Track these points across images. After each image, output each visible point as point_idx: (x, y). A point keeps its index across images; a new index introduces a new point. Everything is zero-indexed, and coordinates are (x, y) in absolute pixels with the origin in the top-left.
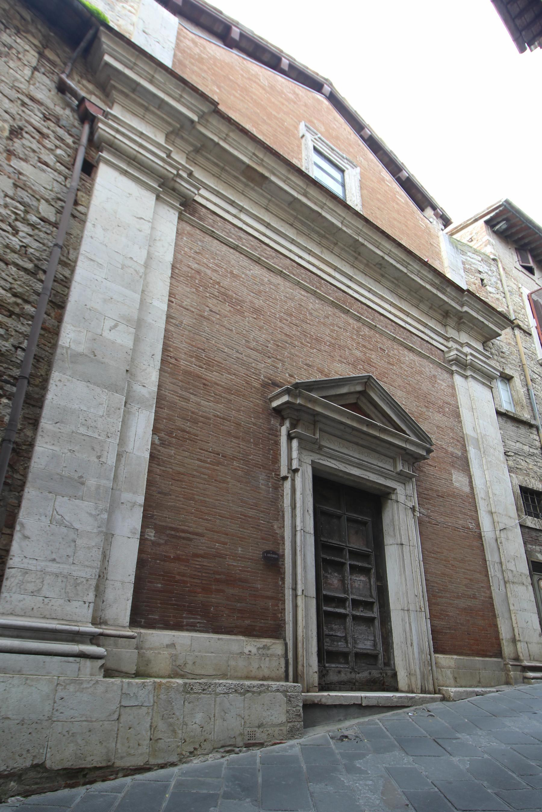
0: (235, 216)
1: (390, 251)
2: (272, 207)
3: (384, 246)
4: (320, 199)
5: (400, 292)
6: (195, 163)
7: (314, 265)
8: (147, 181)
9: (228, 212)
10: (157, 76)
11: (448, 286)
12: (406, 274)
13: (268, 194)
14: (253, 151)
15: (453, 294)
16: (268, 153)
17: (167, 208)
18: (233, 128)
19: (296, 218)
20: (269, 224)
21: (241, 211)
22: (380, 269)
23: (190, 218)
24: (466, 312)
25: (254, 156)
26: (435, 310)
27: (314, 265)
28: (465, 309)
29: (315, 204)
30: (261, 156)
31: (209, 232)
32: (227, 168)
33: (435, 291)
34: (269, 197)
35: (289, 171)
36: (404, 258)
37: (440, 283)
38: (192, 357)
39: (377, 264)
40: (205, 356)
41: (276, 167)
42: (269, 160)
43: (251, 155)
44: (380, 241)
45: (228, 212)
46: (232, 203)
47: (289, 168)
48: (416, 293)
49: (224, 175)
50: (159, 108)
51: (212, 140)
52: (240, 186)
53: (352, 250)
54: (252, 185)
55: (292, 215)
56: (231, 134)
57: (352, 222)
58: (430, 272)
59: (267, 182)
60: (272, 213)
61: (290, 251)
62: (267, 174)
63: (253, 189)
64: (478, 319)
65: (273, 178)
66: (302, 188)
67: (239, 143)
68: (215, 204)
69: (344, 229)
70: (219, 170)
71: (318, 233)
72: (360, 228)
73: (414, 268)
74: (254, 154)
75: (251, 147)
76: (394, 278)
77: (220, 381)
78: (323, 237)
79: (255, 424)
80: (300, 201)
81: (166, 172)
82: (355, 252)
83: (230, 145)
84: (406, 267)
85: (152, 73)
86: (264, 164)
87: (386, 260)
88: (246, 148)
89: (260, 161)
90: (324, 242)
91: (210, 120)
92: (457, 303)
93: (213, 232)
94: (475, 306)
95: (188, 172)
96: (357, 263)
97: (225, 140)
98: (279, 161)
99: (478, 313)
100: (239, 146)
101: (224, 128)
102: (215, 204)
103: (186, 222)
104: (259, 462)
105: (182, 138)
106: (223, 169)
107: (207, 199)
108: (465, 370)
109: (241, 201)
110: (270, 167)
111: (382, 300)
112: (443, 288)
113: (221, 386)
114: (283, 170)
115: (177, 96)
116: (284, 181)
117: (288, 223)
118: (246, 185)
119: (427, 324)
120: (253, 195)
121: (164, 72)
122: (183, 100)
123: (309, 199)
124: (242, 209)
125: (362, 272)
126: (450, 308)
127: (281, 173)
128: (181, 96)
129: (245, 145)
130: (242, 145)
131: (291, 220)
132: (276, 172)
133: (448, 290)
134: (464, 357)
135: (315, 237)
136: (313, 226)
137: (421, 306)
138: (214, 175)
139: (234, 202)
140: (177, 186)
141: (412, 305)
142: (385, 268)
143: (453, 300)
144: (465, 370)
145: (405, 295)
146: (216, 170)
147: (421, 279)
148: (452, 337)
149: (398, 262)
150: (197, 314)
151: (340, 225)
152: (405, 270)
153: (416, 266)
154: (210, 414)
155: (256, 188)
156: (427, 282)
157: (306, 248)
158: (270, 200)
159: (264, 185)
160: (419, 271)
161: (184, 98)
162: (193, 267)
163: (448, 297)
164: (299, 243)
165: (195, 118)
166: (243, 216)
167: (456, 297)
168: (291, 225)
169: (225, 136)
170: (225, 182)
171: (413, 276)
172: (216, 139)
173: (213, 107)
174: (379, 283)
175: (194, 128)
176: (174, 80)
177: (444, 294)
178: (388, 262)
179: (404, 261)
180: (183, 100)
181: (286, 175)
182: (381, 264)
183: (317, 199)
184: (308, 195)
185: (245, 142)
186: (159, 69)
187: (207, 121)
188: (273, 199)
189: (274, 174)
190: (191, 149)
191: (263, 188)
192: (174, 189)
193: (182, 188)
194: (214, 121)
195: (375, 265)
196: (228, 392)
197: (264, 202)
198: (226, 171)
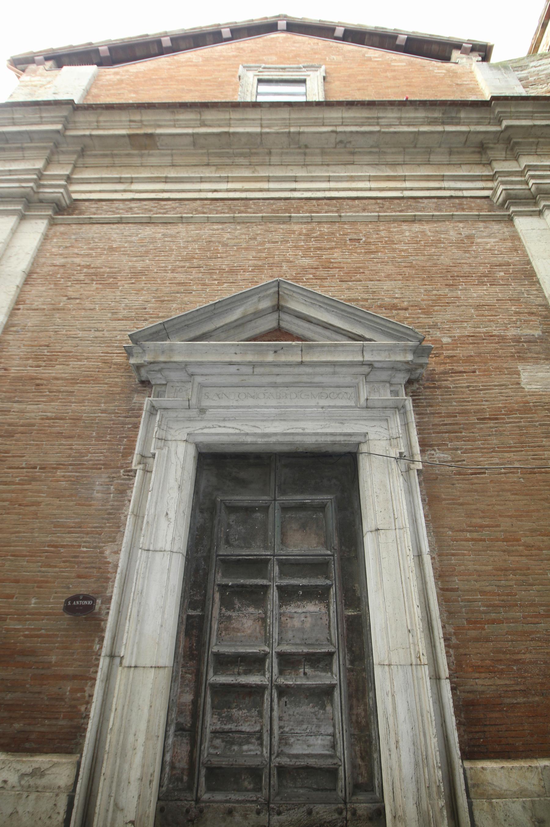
0: (125, 191)
1: (342, 118)
2: (178, 160)
3: (331, 118)
4: (222, 117)
5: (389, 158)
6: (87, 167)
7: (235, 190)
8: (5, 208)
9: (116, 191)
10: (16, 116)
11: (458, 112)
12: (379, 132)
13: (168, 149)
14: (128, 119)
15: (474, 115)
16: (143, 111)
17: (33, 221)
18: (99, 111)
19: (208, 154)
20: (166, 178)
21: (132, 182)
22: (345, 147)
23: (63, 219)
24: (507, 127)
25: (132, 124)
26: (459, 153)
27: (235, 190)
28: (505, 123)
29: (220, 126)
30: (137, 118)
31: (87, 221)
32: (115, 152)
33: (440, 128)
34: (169, 152)
35: (173, 112)
36: (366, 115)
37: (443, 114)
38: (28, 359)
39: (337, 144)
40: (48, 352)
41: (158, 118)
42: (148, 116)
43: (128, 123)
44: (321, 116)
45: (116, 191)
46: (120, 181)
47: (170, 110)
48: (415, 147)
49: (117, 161)
50: (32, 140)
51: (84, 136)
52: (137, 161)
53: (295, 148)
54: (146, 152)
55: (202, 154)
56: (101, 119)
57: (274, 117)
58: (416, 109)
59: (157, 139)
60: (180, 166)
61: (200, 191)
62: (149, 131)
63: (149, 155)
64: (535, 126)
65: (159, 131)
66: (196, 120)
67: (112, 121)
68: (100, 191)
69: (267, 130)
70: (110, 159)
71: (242, 155)
72: (287, 116)
73: (390, 118)
74: (131, 121)
75: (124, 117)
76: (372, 147)
77: (63, 373)
78: (251, 154)
79: (103, 411)
80: (198, 134)
81: (23, 190)
82: (300, 148)
83: (104, 129)
84: (378, 124)
85: (10, 116)
86: (145, 123)
87: (341, 132)
88: (121, 121)
89: (139, 124)
90: (254, 159)
91: (77, 119)
92: (489, 124)
93: (90, 218)
94: (521, 112)
95: (65, 178)
96: (309, 159)
97: (98, 128)
98: (157, 111)
99: (532, 118)
100: (112, 124)
101: (91, 117)
102: (100, 191)
103: (61, 224)
104: (100, 460)
105: (63, 153)
106: (113, 156)
107: (90, 192)
108: (536, 204)
109: (141, 173)
110: (152, 123)
111: (354, 181)
112: (452, 118)
113: (62, 379)
114: (167, 116)
115: (39, 120)
116: (174, 126)
117: (203, 166)
118: (142, 156)
119: (443, 176)
120: (153, 160)
121: (18, 108)
122: (44, 120)
123: (210, 126)
124: (132, 181)
125: (322, 165)
126: (481, 137)
127: (165, 120)
128: (41, 117)
129: (117, 118)
130: (115, 121)
131: (205, 160)
132: (160, 123)
133: (462, 115)
134: (524, 187)
135: (241, 160)
136: (231, 151)
137: (434, 158)
138: (107, 167)
139: (121, 178)
140: (41, 196)
141: (419, 165)
142: (350, 142)
143: (478, 124)
144: (536, 204)
145: (400, 158)
146: (107, 161)
147: (409, 125)
148: (496, 172)
149: (362, 125)
150: (49, 310)
151: (258, 130)
152: (377, 129)
153: (391, 114)
154: (35, 419)
155: (151, 152)
156: (422, 124)
157: (220, 177)
158: (172, 155)
159: (158, 144)
160: (400, 118)
161: (45, 117)
162: (58, 264)
163: (468, 124)
164: (209, 177)
165: (59, 127)
166: (135, 187)
167: (482, 118)
168: (208, 165)
169: (96, 124)
170: (120, 166)
171: (392, 130)
172: (87, 133)
173: (71, 106)
174: (353, 164)
175: (65, 136)
176: (29, 109)
177: (458, 124)
178: (345, 132)
179: (369, 118)
180: (44, 120)
181: (172, 118)
182: (341, 142)
183: (218, 120)
184: (206, 123)
185: (117, 116)
186: (14, 108)
187: (75, 122)
188: (174, 151)
189: (160, 126)
190: (74, 157)
191: (160, 148)
192: (41, 201)
193: (47, 195)
194: (81, 117)
195: (335, 148)
196: (71, 383)
197: (167, 160)
198: (116, 155)
